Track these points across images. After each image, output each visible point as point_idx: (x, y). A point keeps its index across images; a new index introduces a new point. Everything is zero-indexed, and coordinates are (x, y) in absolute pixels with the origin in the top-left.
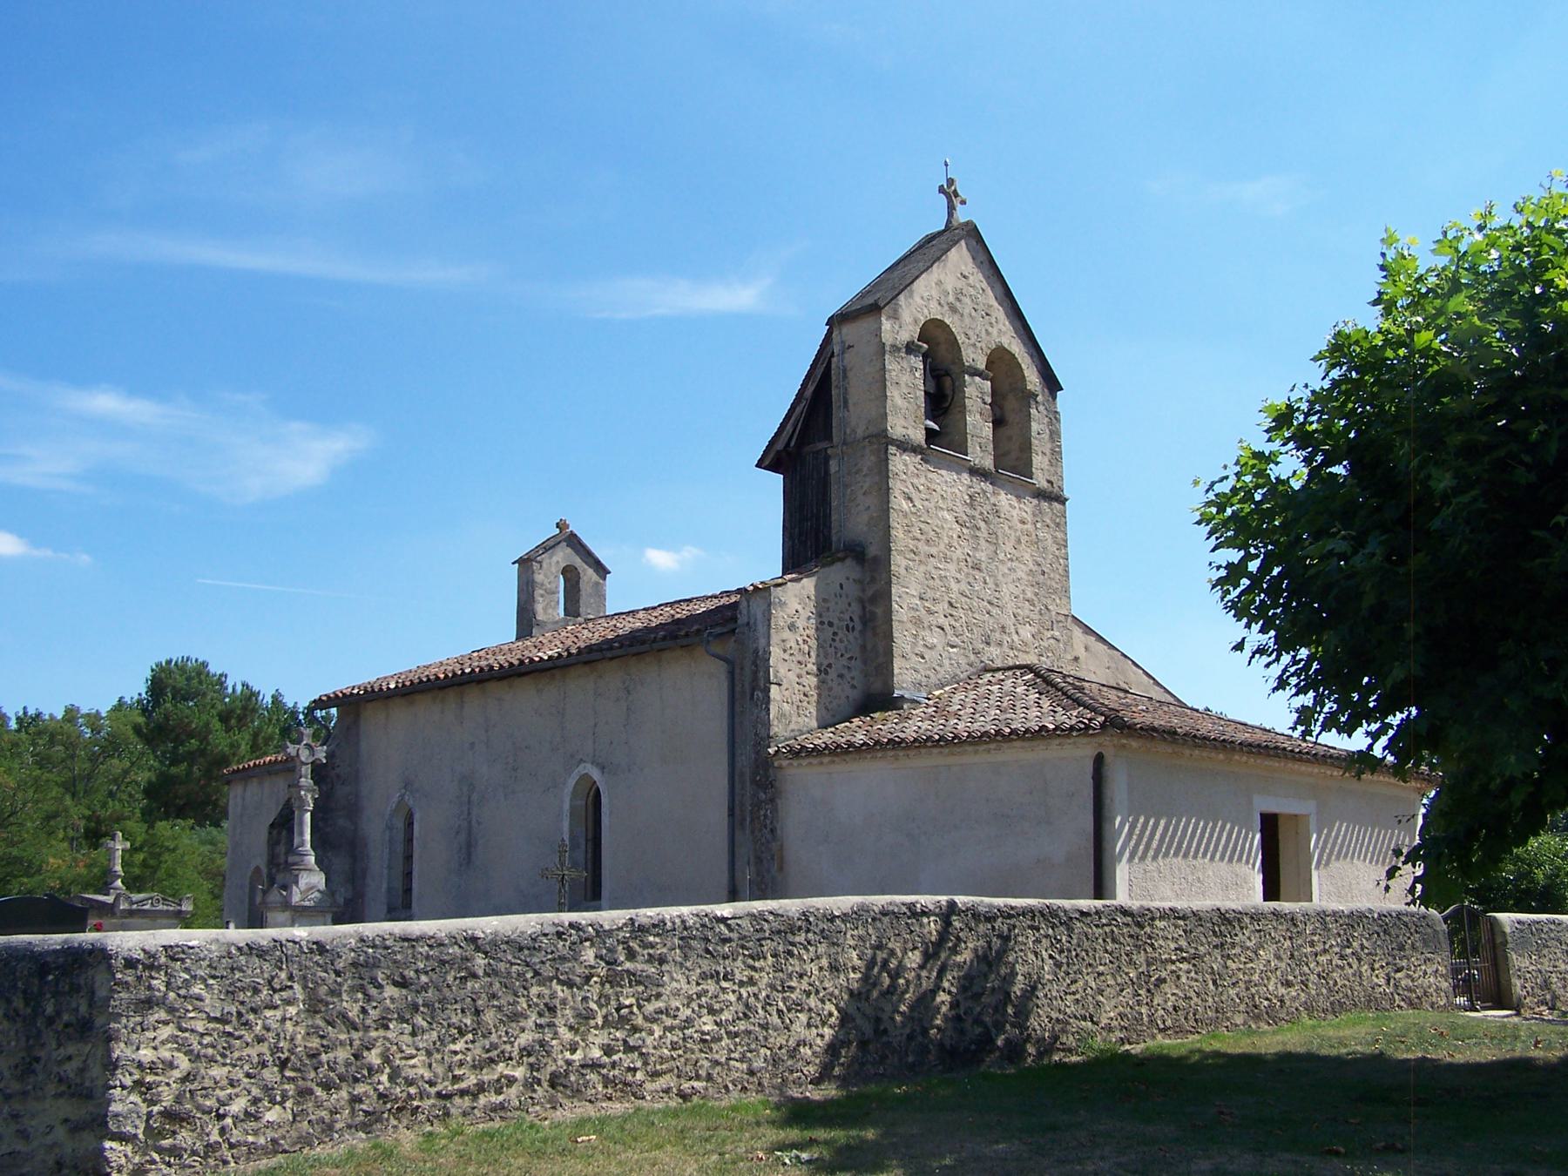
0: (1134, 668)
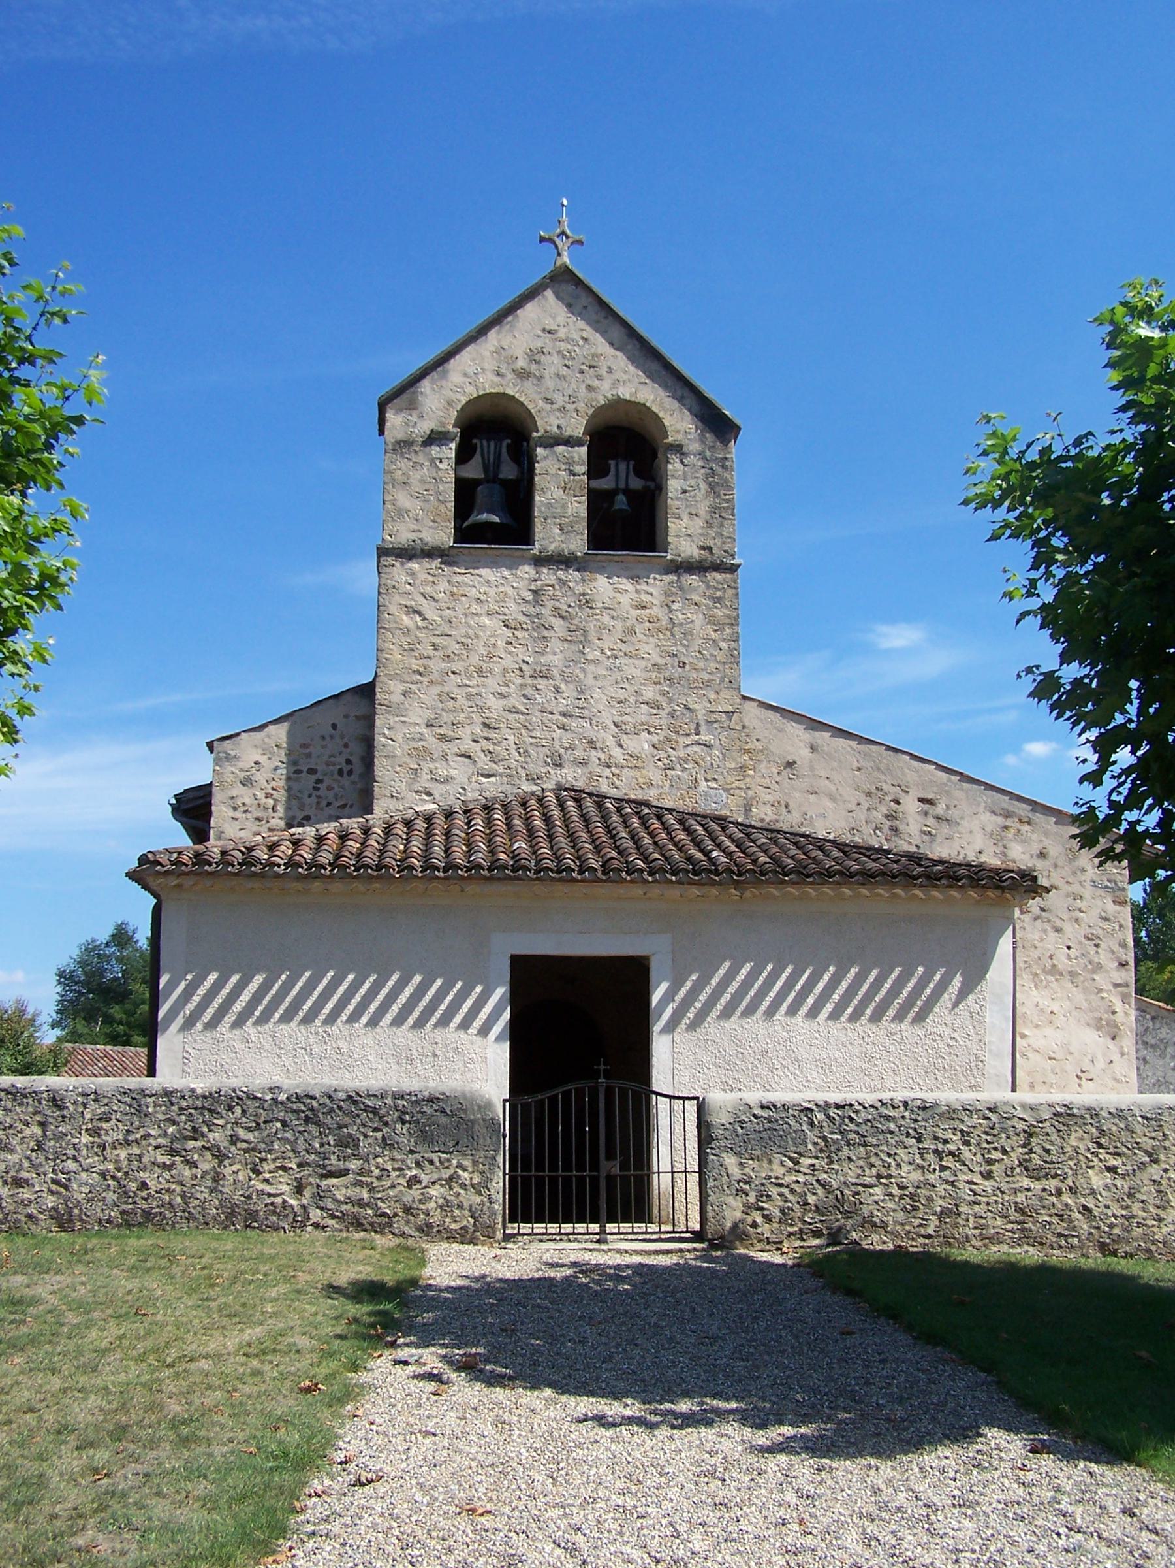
0: (915, 764)
